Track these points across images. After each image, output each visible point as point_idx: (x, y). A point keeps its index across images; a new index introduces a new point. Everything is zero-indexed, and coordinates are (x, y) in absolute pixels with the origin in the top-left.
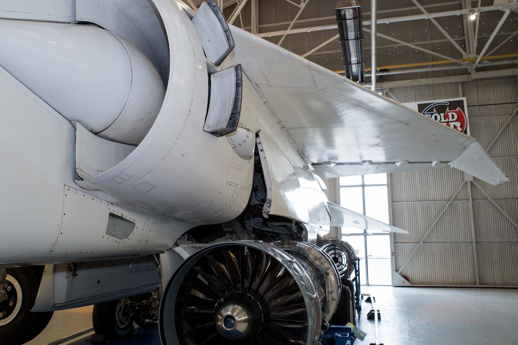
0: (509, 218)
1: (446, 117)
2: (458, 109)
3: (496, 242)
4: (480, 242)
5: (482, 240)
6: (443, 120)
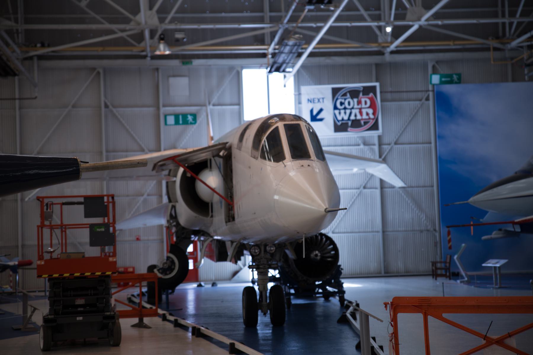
1: (359, 103)
2: (371, 95)
3: (401, 231)
6: (356, 106)
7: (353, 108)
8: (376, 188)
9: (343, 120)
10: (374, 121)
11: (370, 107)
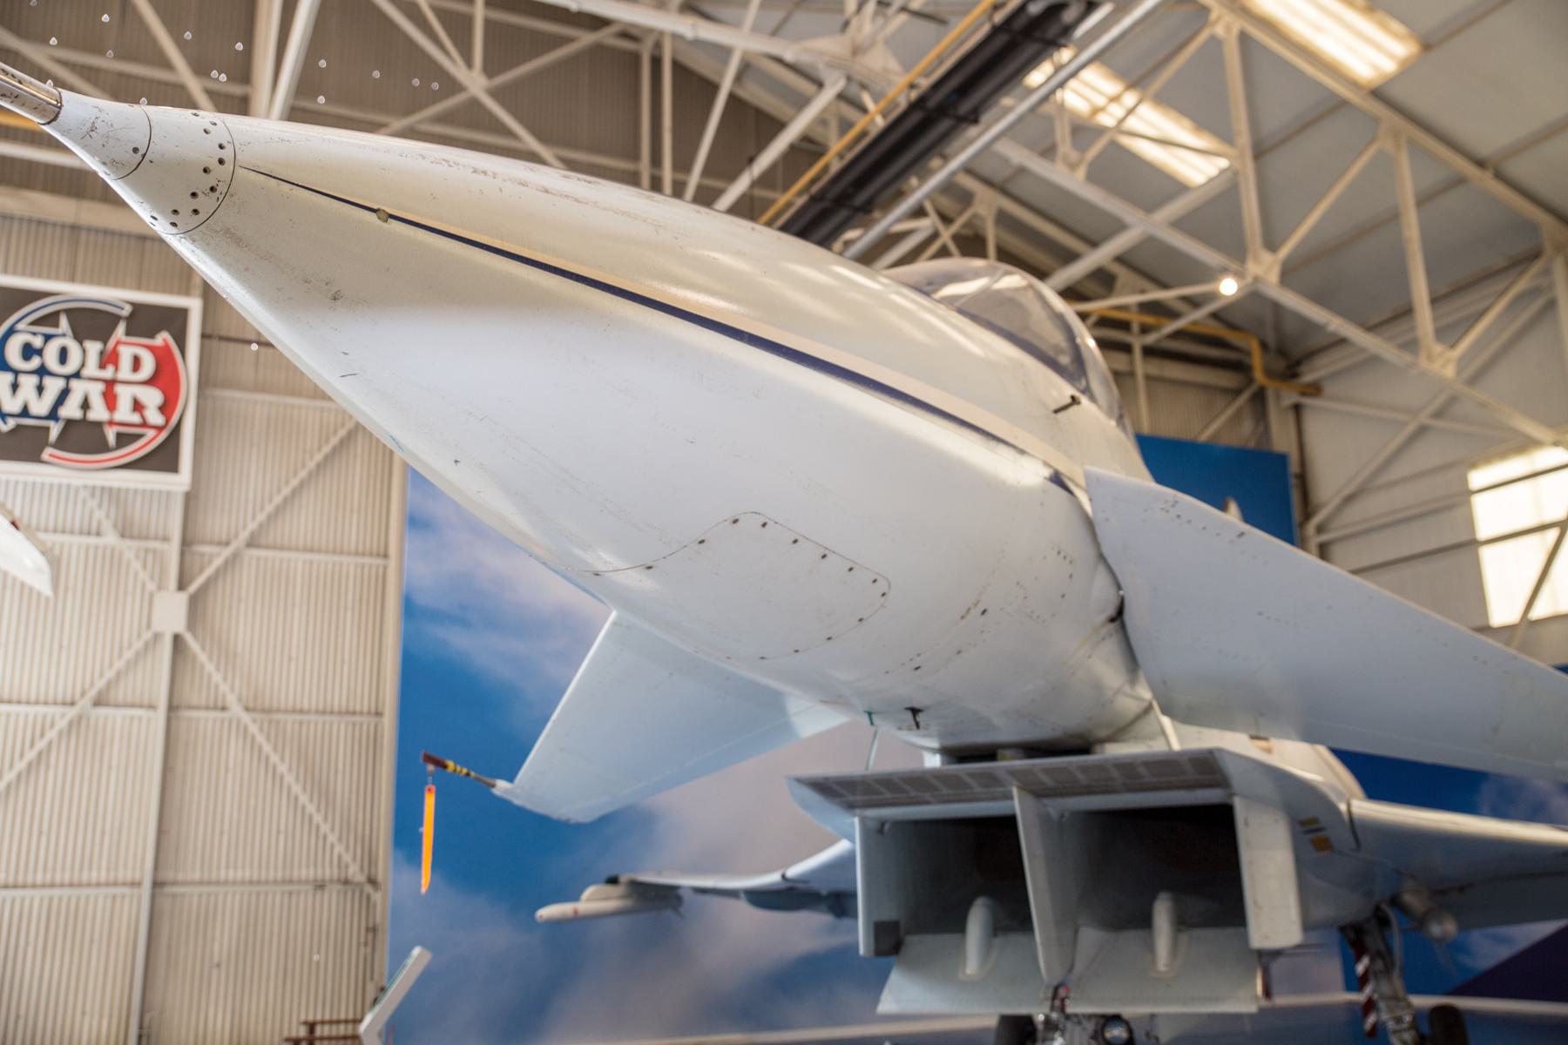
0: (297, 789)
1: (109, 359)
2: (163, 338)
3: (234, 883)
4: (175, 883)
5: (180, 876)
6: (91, 369)
7: (77, 375)
8: (152, 707)
9: (25, 412)
10: (164, 435)
11: (150, 382)
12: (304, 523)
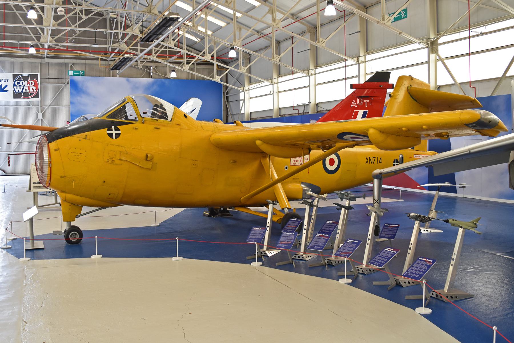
1: (28, 83)
6: (26, 85)
9: (19, 91)
12: (57, 102)
